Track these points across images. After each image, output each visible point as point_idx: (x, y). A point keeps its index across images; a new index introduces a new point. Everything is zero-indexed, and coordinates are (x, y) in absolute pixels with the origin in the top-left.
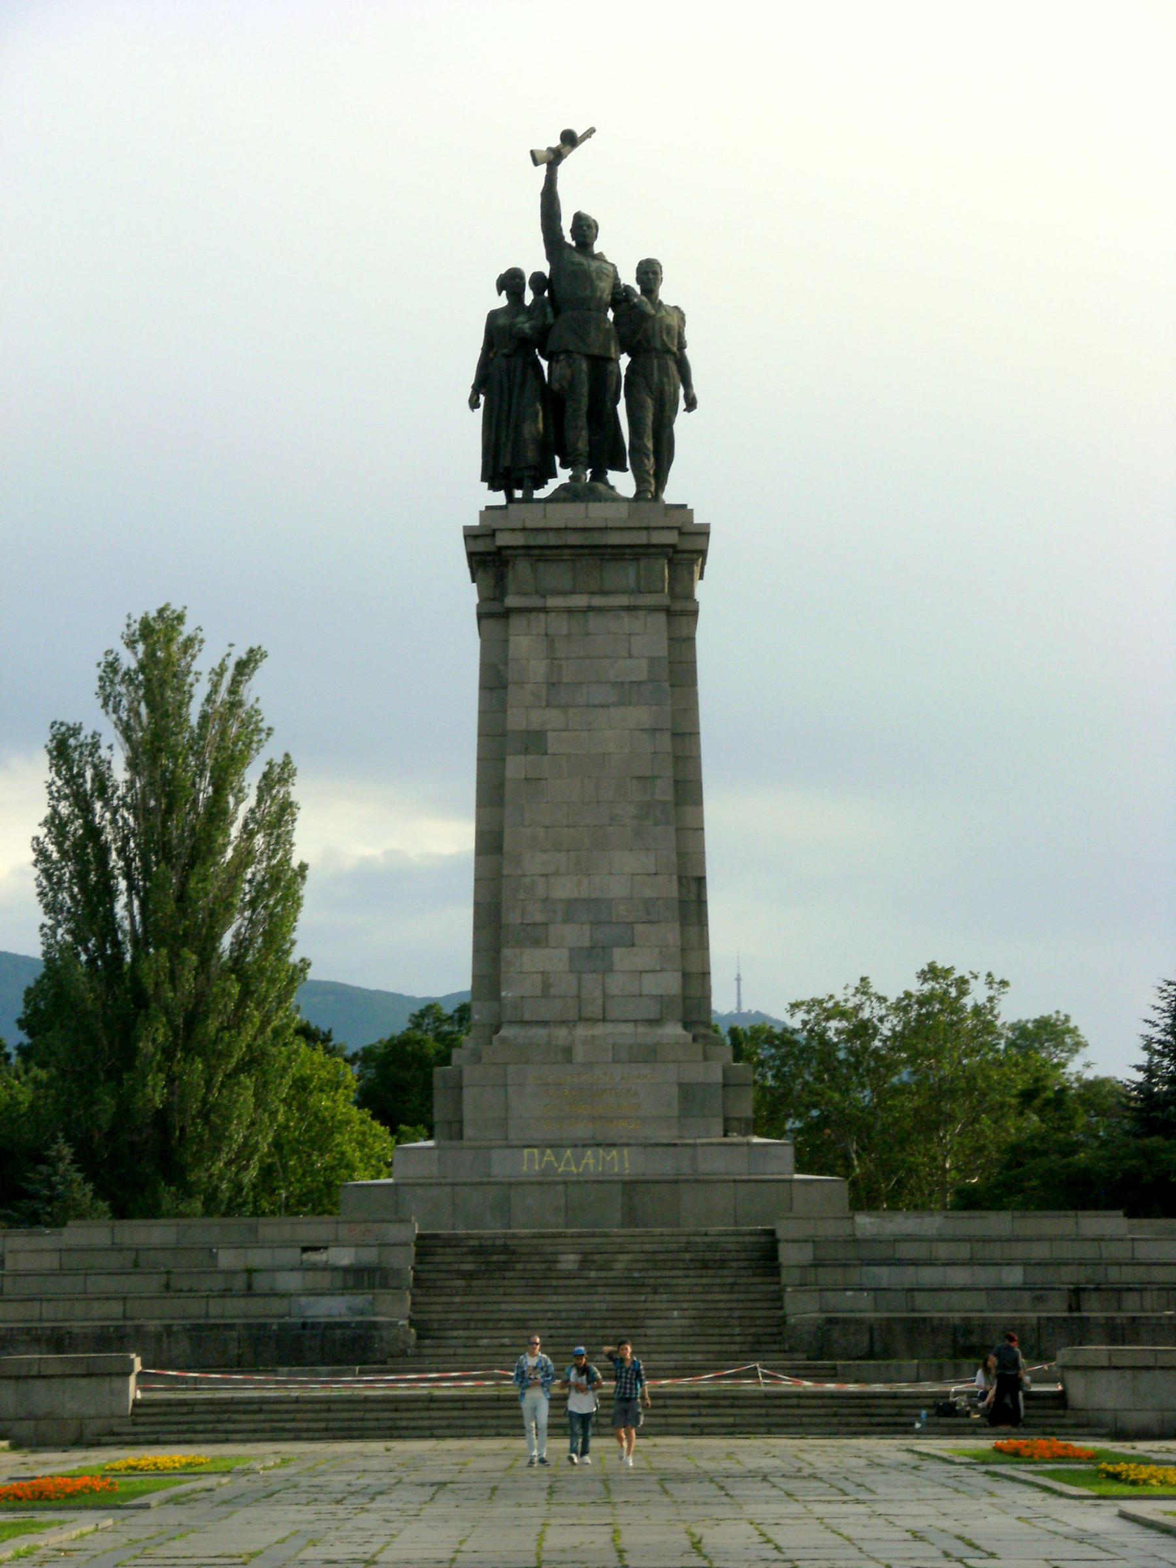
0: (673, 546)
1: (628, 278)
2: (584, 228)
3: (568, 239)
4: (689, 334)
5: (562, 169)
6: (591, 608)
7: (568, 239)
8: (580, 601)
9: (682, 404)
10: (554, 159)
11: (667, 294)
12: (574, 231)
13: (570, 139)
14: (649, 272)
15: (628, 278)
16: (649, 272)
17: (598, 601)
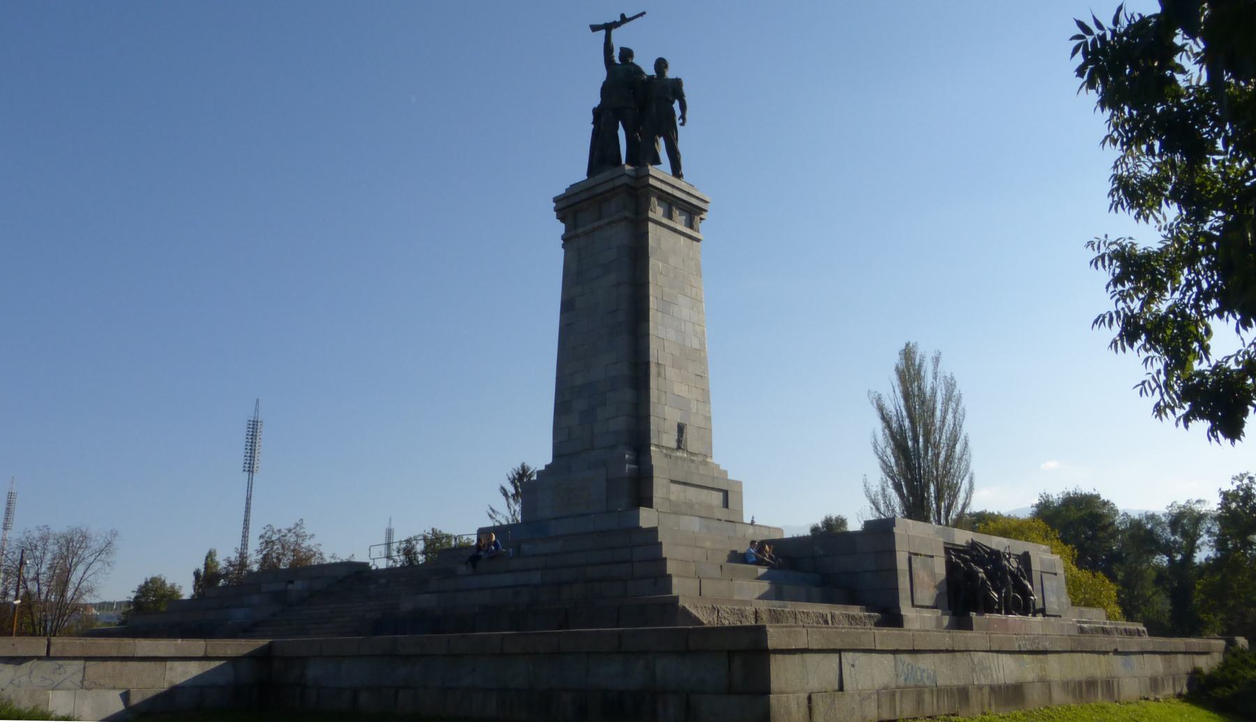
0: (625, 185)
1: (649, 70)
2: (627, 54)
3: (617, 61)
4: (684, 88)
5: (614, 32)
6: (594, 229)
7: (617, 61)
8: (589, 227)
9: (678, 122)
10: (609, 27)
11: (670, 74)
12: (621, 58)
13: (624, 20)
14: (661, 65)
15: (649, 70)
16: (661, 65)
17: (596, 224)
